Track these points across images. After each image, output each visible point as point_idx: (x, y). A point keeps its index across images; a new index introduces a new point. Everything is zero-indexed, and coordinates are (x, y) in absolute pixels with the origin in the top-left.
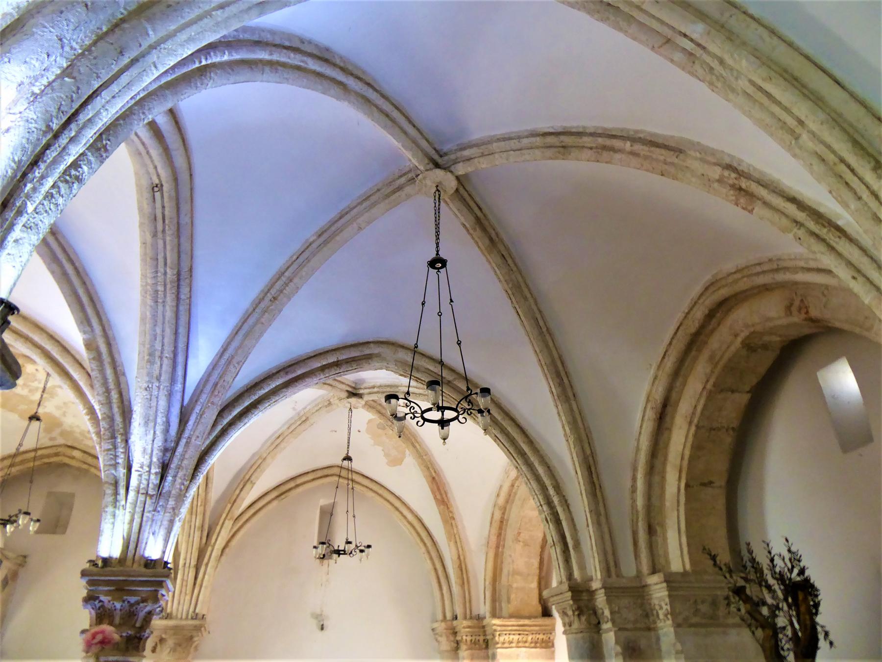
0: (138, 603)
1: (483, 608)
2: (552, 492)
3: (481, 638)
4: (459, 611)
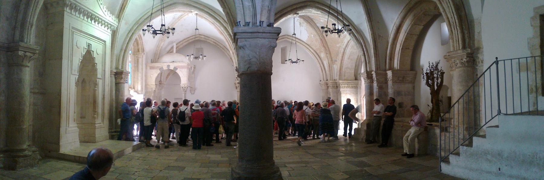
1: (336, 77)
4: (329, 79)
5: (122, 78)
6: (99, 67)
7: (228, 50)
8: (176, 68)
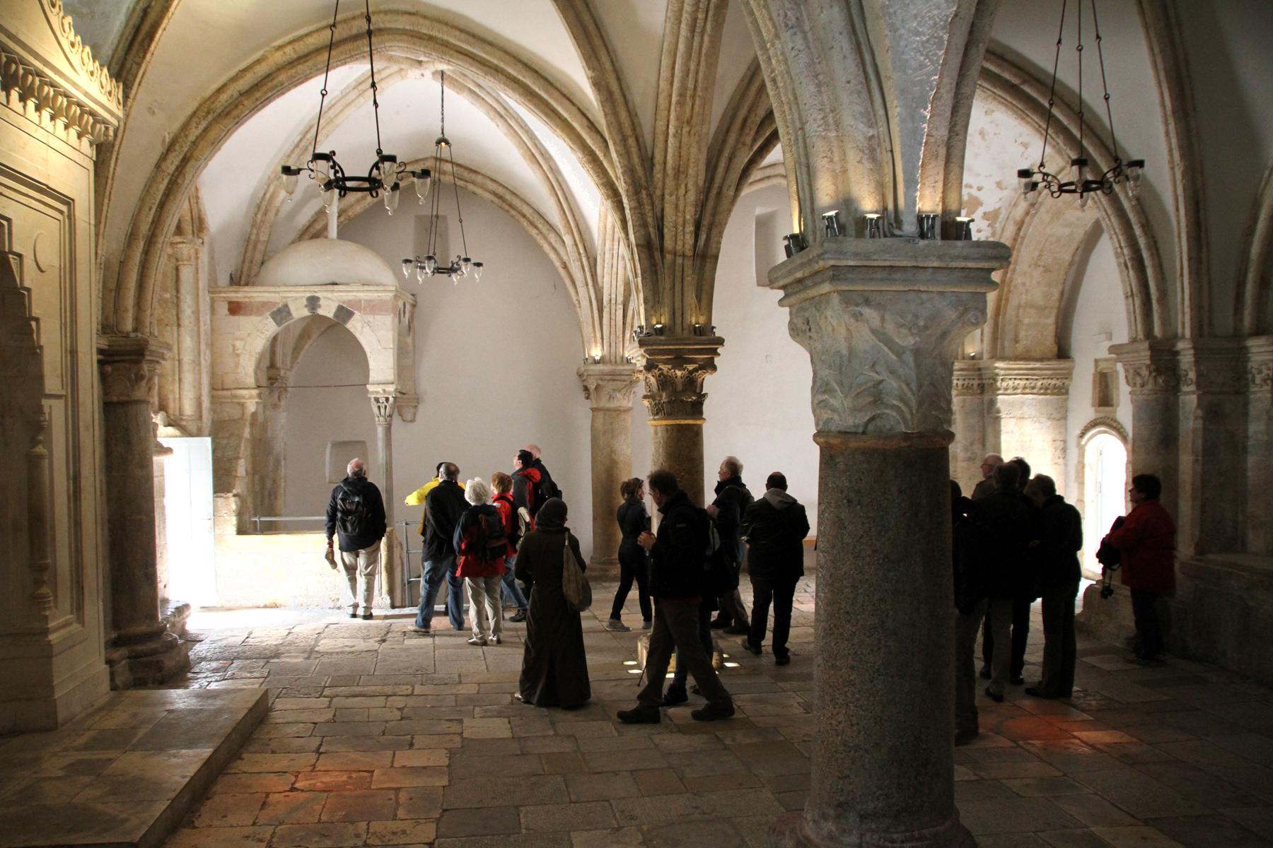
0: (696, 370)
2: (1138, 231)
3: (976, 382)
5: (140, 378)
6: (50, 337)
7: (552, 228)
8: (344, 313)
